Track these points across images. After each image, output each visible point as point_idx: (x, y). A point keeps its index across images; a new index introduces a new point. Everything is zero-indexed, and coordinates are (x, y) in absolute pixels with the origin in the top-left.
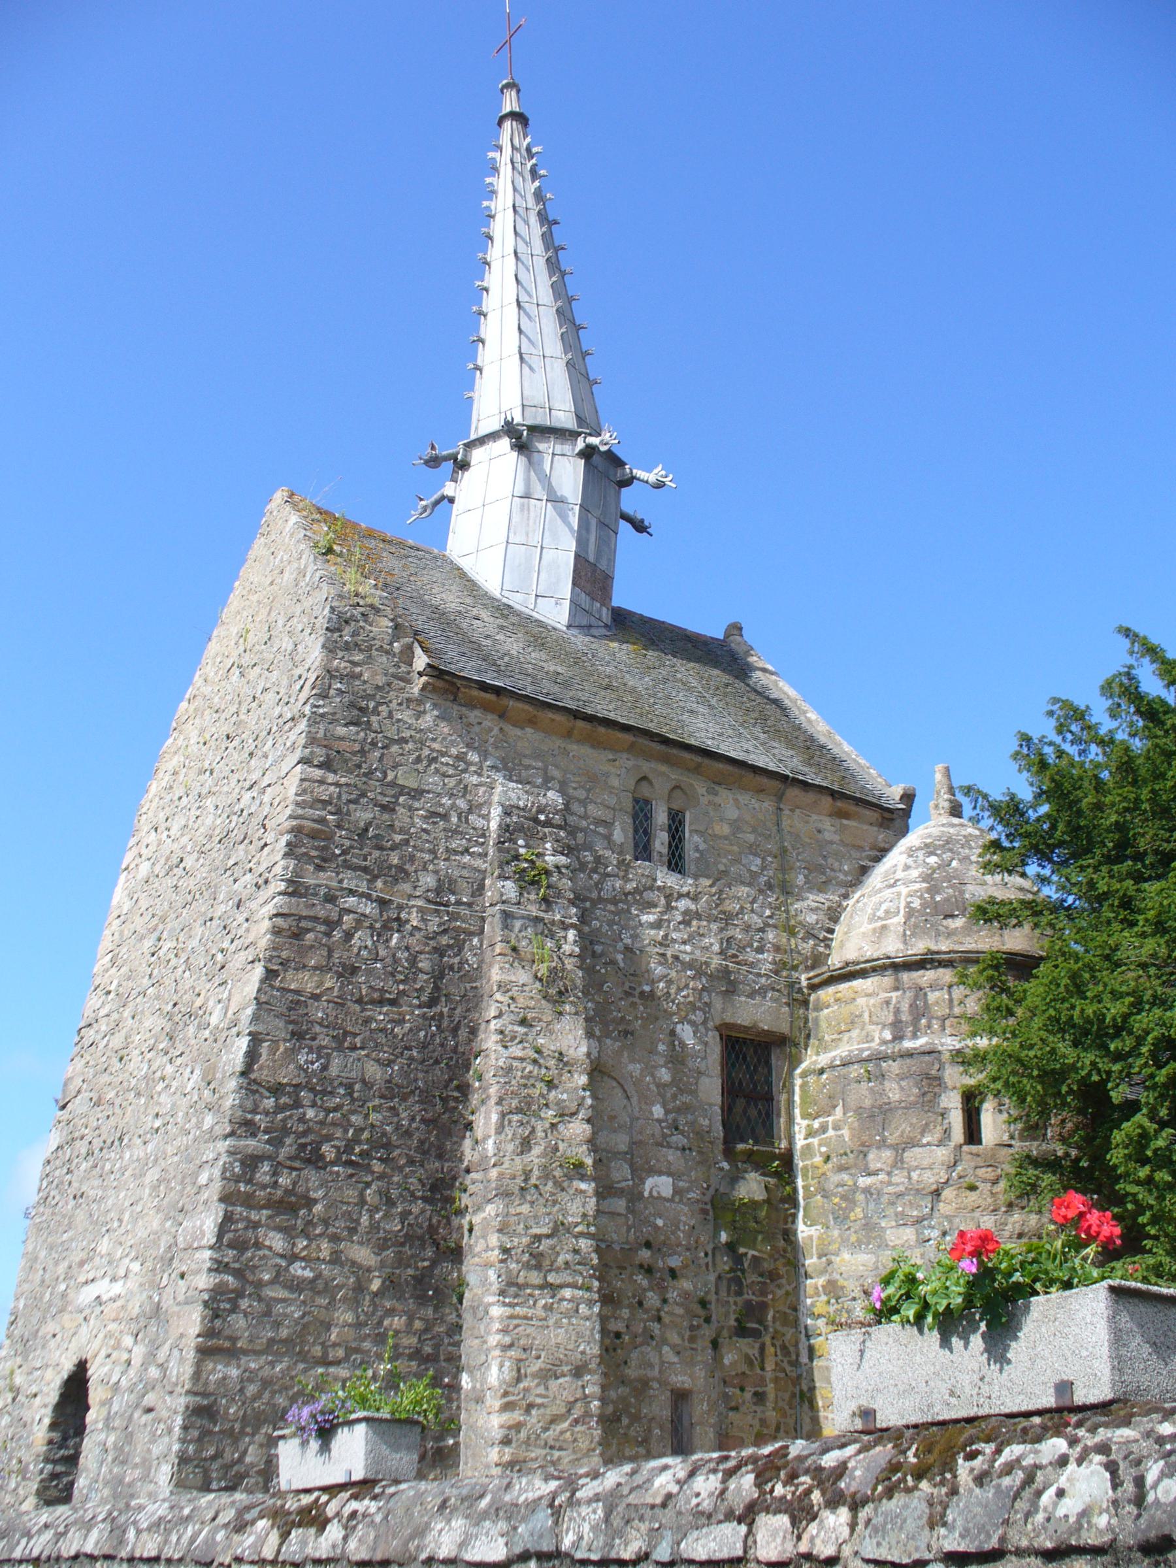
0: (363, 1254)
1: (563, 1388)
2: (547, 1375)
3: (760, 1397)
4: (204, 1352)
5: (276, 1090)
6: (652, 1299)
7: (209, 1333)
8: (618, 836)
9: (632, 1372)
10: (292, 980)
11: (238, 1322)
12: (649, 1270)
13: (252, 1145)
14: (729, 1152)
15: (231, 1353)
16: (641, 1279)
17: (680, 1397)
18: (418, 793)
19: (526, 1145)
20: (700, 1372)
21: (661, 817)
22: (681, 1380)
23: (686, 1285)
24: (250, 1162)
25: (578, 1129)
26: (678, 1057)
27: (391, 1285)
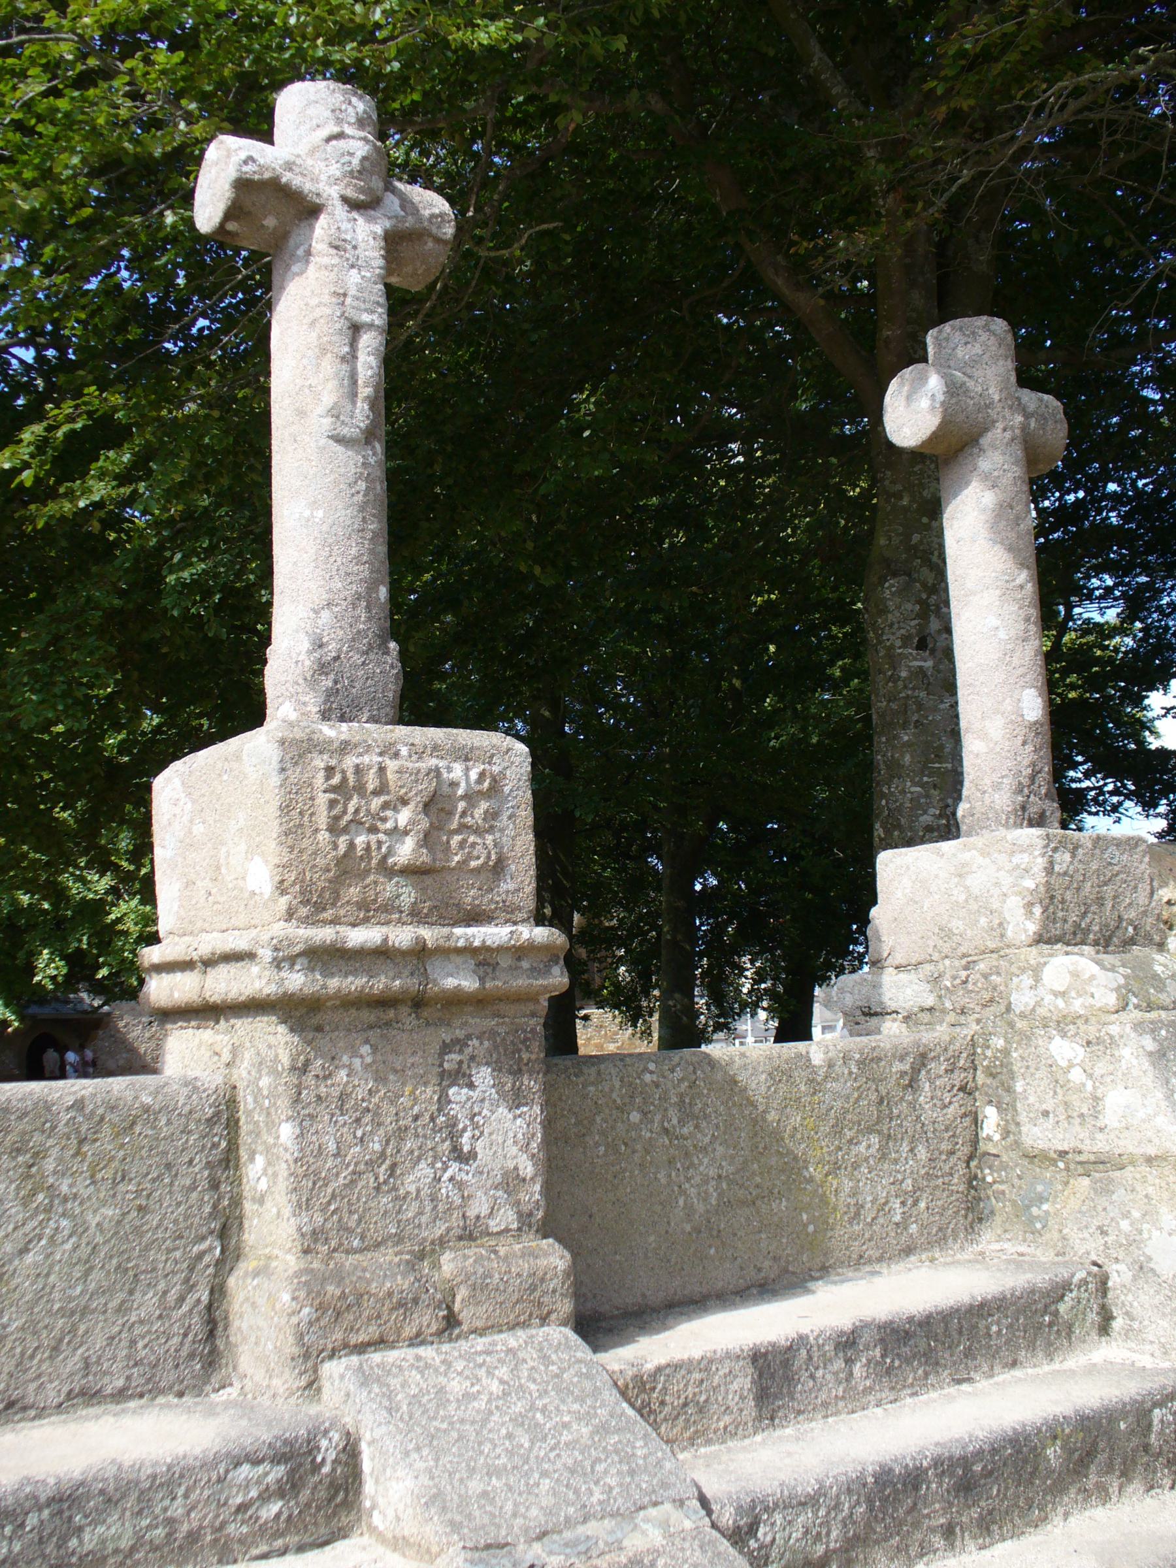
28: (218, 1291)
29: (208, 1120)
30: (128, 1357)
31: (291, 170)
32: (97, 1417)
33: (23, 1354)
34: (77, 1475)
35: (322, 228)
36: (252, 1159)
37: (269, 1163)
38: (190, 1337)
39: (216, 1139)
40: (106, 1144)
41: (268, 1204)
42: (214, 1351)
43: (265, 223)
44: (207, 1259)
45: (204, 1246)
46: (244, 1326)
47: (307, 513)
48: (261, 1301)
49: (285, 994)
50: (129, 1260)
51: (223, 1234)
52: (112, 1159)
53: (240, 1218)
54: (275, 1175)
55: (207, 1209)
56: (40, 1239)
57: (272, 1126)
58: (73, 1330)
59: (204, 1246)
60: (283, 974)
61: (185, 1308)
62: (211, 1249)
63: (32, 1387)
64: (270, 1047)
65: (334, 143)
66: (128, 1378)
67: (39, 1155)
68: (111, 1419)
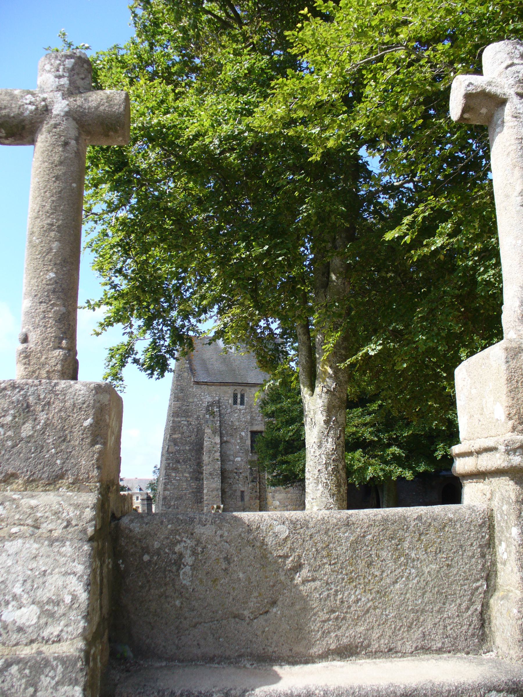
0: (187, 475)
1: (215, 493)
2: (212, 491)
3: (256, 492)
4: (164, 490)
5: (172, 453)
6: (237, 477)
7: (165, 488)
8: (230, 402)
9: (234, 489)
10: (174, 436)
11: (169, 486)
12: (236, 473)
13: (169, 461)
14: (252, 453)
15: (168, 490)
16: (235, 474)
17: (242, 492)
18: (193, 402)
19: (209, 457)
20: (246, 488)
21: (239, 396)
22: (242, 489)
23: (243, 474)
24: (169, 464)
25: (218, 454)
26: (241, 438)
27: (191, 478)
28: (485, 606)
29: (479, 525)
30: (443, 633)
31: (490, 85)
32: (428, 660)
33: (395, 628)
34: (414, 686)
35: (508, 109)
36: (500, 544)
37: (508, 546)
38: (472, 627)
39: (484, 534)
40: (432, 535)
41: (508, 565)
42: (484, 634)
43: (482, 111)
44: (480, 590)
45: (479, 584)
46: (497, 623)
47: (514, 242)
48: (504, 612)
49: (512, 466)
50: (443, 589)
51: (488, 579)
52: (435, 542)
53: (496, 572)
54: (510, 552)
55: (480, 567)
56: (402, 578)
57: (508, 528)
58: (418, 619)
59: (479, 584)
60: (510, 457)
61: (470, 612)
62: (482, 585)
63: (399, 643)
64: (506, 491)
65: (509, 68)
66: (443, 643)
67: (401, 540)
68: (434, 661)
